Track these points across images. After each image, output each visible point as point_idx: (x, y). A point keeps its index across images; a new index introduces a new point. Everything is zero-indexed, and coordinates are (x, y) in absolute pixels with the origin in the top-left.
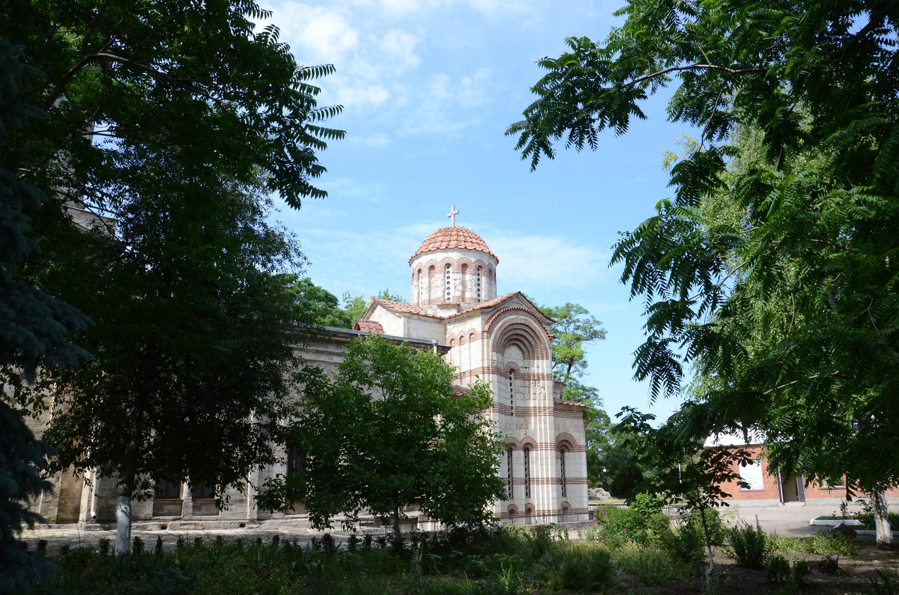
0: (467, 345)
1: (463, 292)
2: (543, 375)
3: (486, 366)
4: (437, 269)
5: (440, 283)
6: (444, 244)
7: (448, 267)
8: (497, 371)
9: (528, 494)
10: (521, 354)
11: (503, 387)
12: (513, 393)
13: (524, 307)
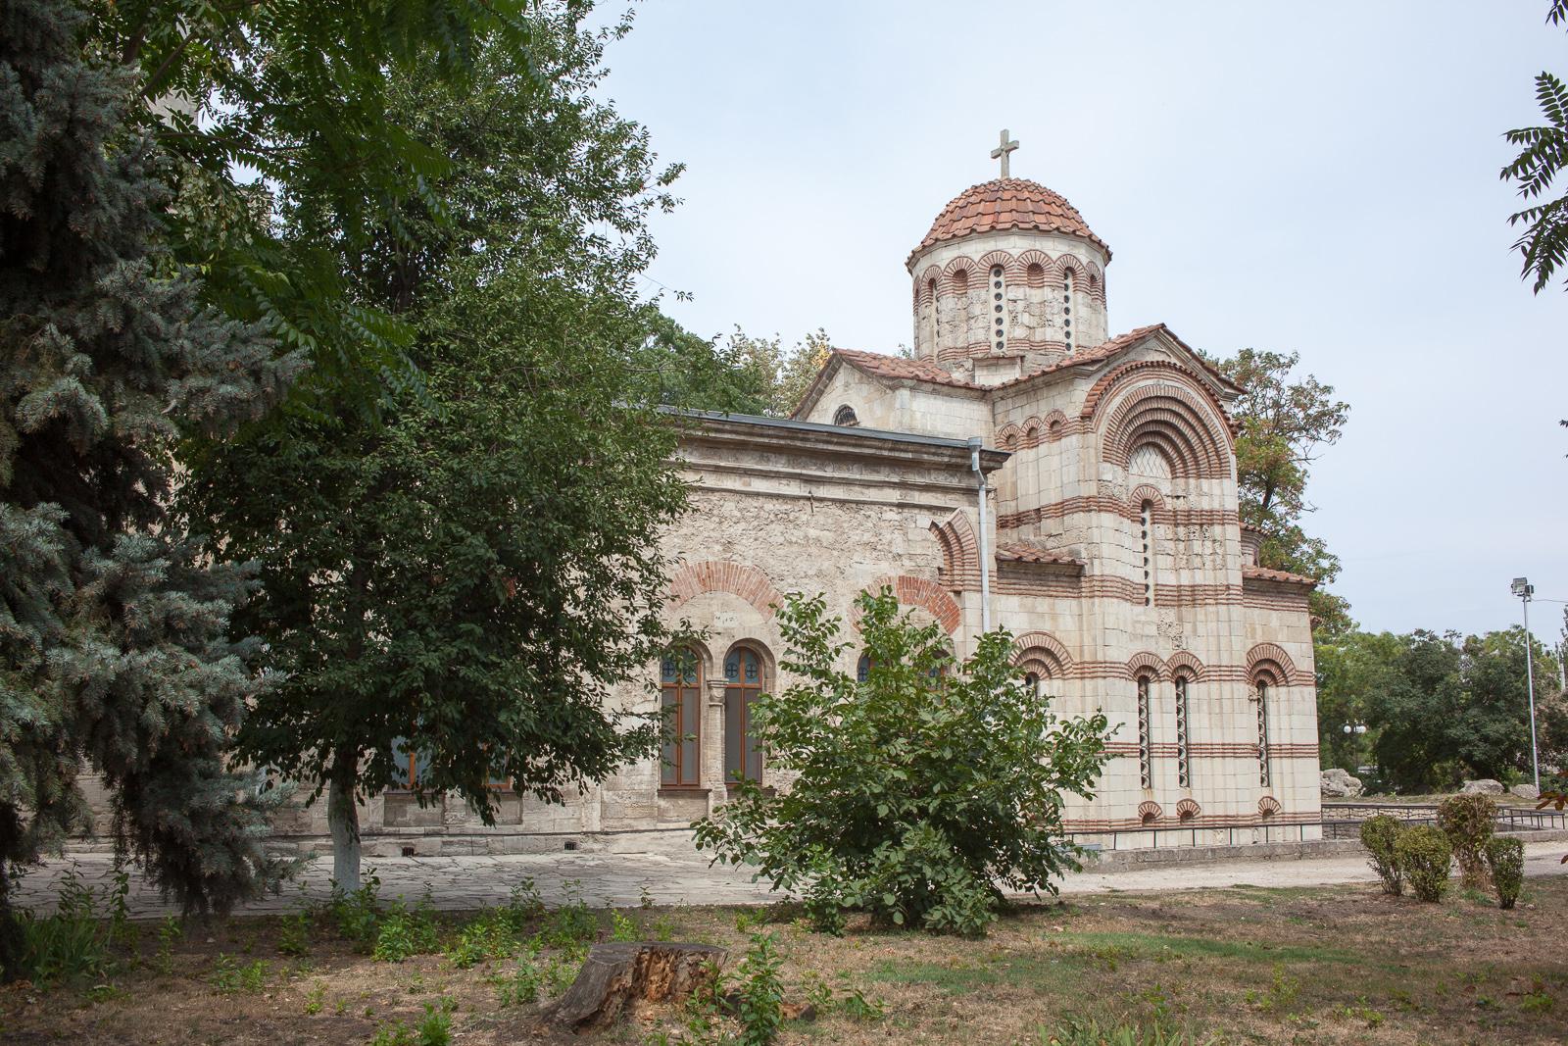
6: (987, 220)
7: (998, 274)
10: (1167, 468)
11: (1128, 542)
12: (1149, 554)
13: (1173, 360)
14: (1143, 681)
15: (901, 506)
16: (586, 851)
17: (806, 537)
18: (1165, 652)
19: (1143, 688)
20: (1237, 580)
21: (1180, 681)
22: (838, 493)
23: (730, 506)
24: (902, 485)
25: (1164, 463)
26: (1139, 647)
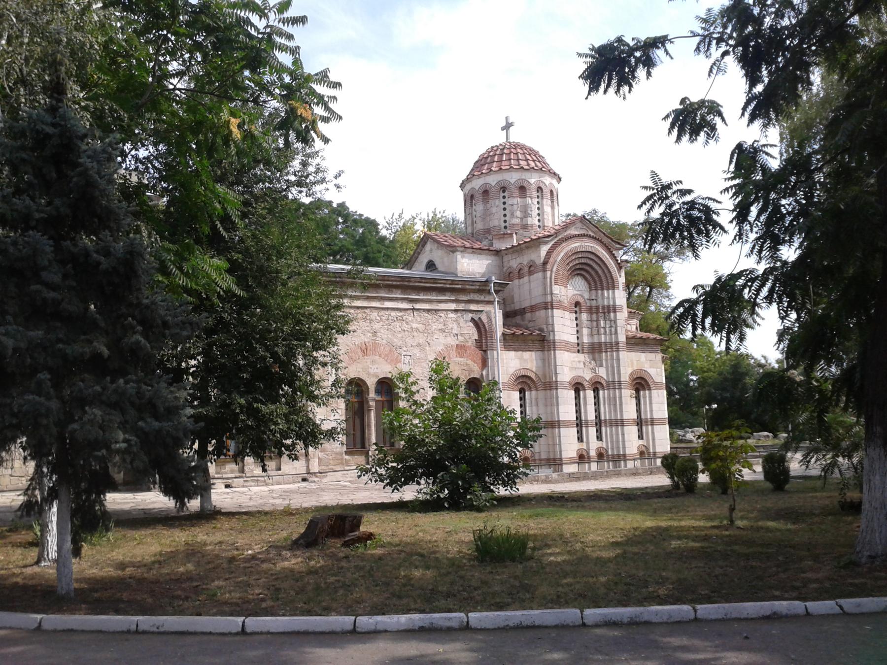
0: (526, 279)
7: (504, 192)
10: (587, 286)
11: (568, 323)
14: (577, 391)
15: (456, 311)
16: (312, 482)
17: (412, 328)
18: (588, 376)
20: (622, 338)
21: (596, 391)
22: (427, 306)
23: (374, 315)
24: (456, 301)
26: (574, 374)
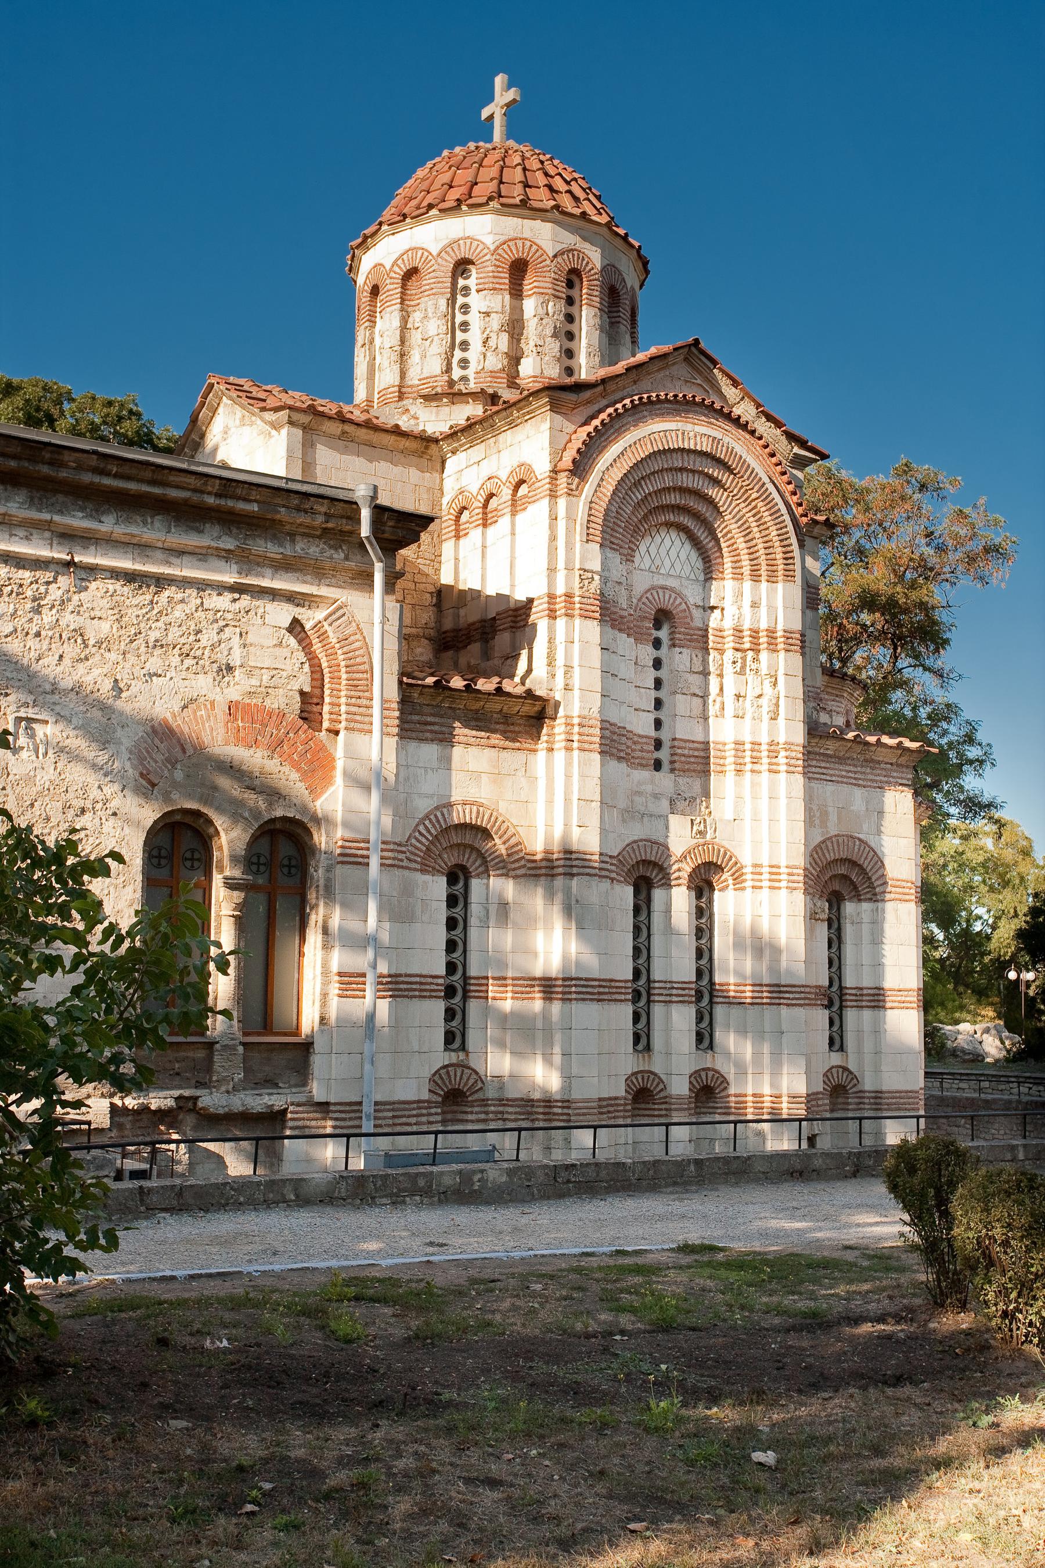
1: (515, 359)
2: (771, 632)
3: (560, 590)
4: (427, 281)
5: (435, 326)
8: (608, 613)
9: (705, 1039)
10: (700, 564)
11: (626, 670)
19: (643, 896)
25: (694, 555)
